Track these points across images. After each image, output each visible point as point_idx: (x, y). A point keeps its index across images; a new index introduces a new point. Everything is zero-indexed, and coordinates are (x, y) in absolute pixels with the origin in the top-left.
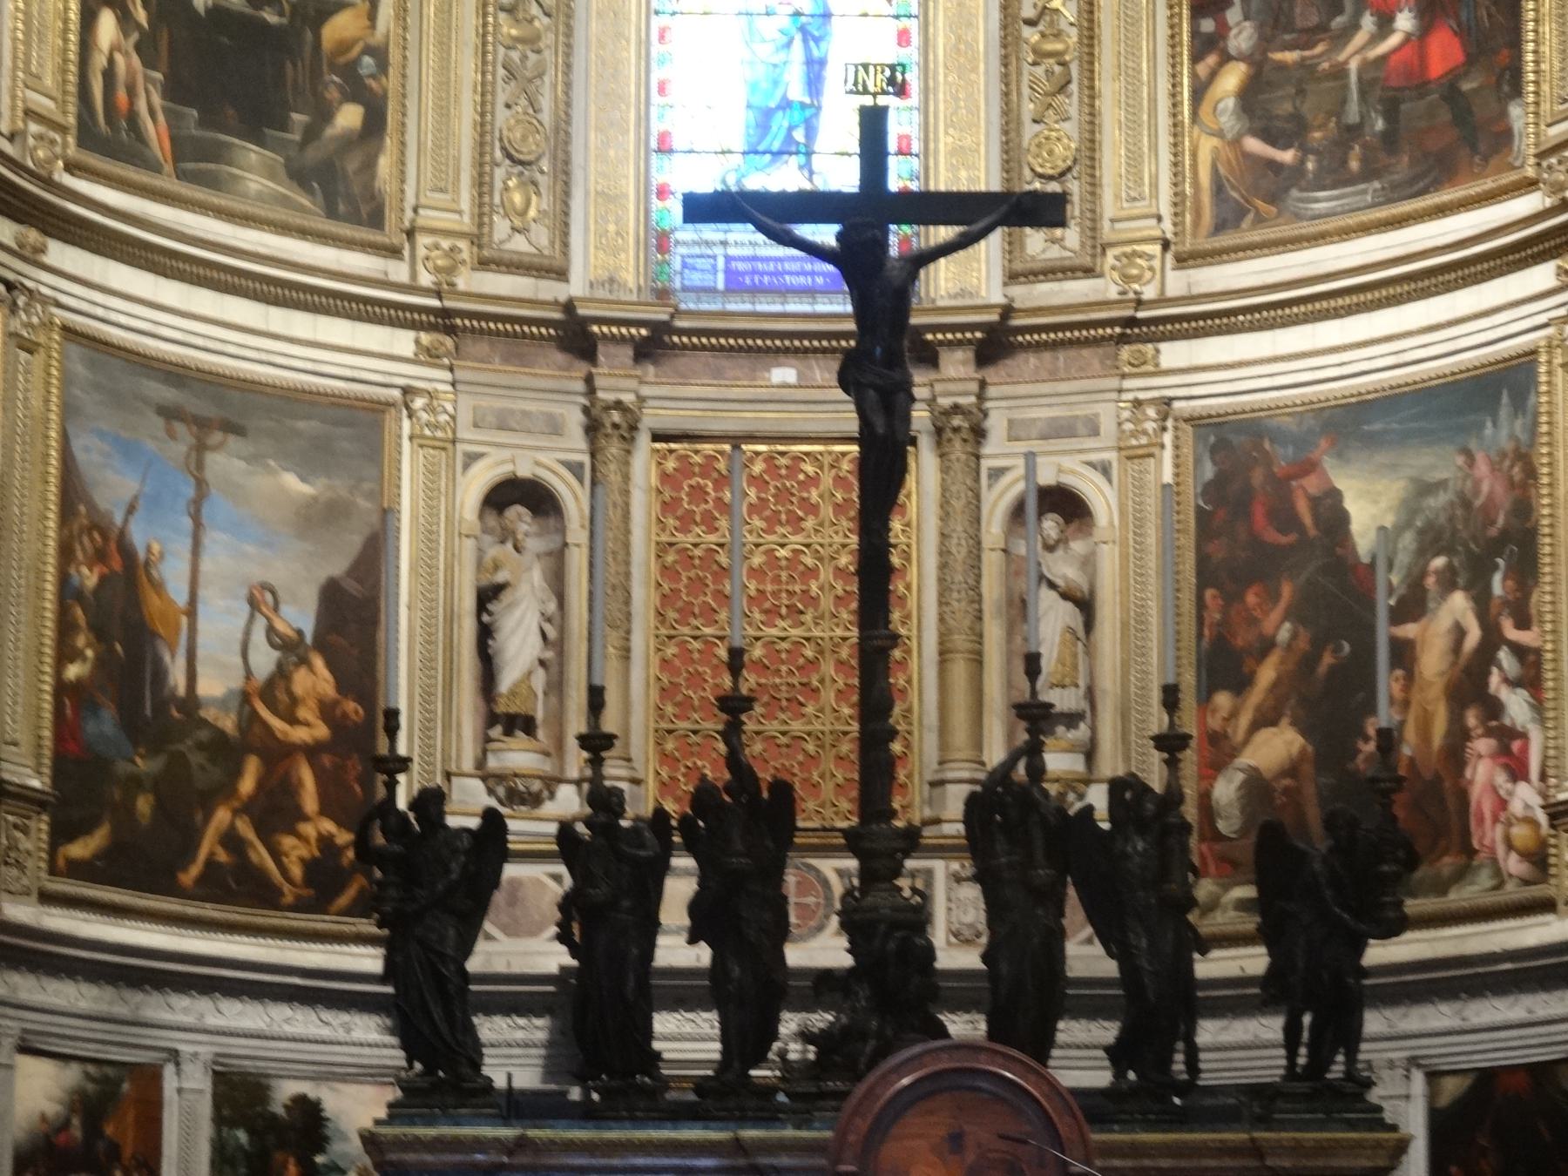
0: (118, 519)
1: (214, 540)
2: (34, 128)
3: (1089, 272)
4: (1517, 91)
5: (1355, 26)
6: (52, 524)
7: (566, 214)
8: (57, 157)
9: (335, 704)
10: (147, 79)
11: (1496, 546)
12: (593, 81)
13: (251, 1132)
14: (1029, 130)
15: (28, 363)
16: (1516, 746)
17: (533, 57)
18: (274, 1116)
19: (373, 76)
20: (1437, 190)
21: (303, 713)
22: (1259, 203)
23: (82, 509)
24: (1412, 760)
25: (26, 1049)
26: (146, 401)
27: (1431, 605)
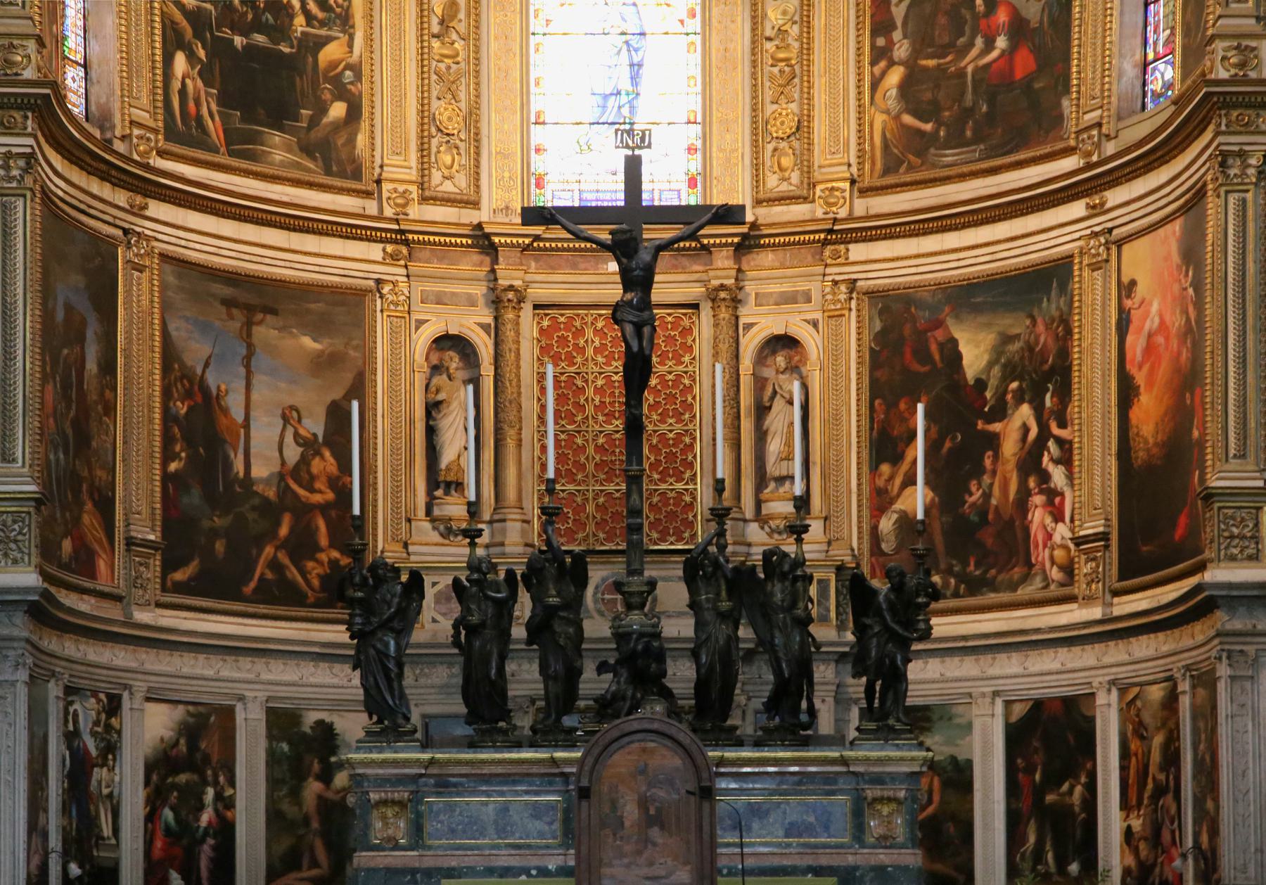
0: (199, 371)
1: (257, 380)
2: (136, 132)
3: (805, 199)
4: (1067, 90)
5: (971, 45)
6: (157, 377)
7: (477, 166)
8: (152, 149)
9: (338, 478)
10: (207, 94)
11: (1048, 376)
12: (493, 81)
13: (290, 743)
14: (770, 108)
15: (139, 278)
16: (1057, 500)
17: (454, 67)
18: (305, 733)
19: (351, 83)
20: (1017, 151)
21: (318, 485)
22: (911, 157)
23: (176, 366)
24: (997, 507)
25: (148, 699)
26: (214, 296)
27: (1010, 412)
